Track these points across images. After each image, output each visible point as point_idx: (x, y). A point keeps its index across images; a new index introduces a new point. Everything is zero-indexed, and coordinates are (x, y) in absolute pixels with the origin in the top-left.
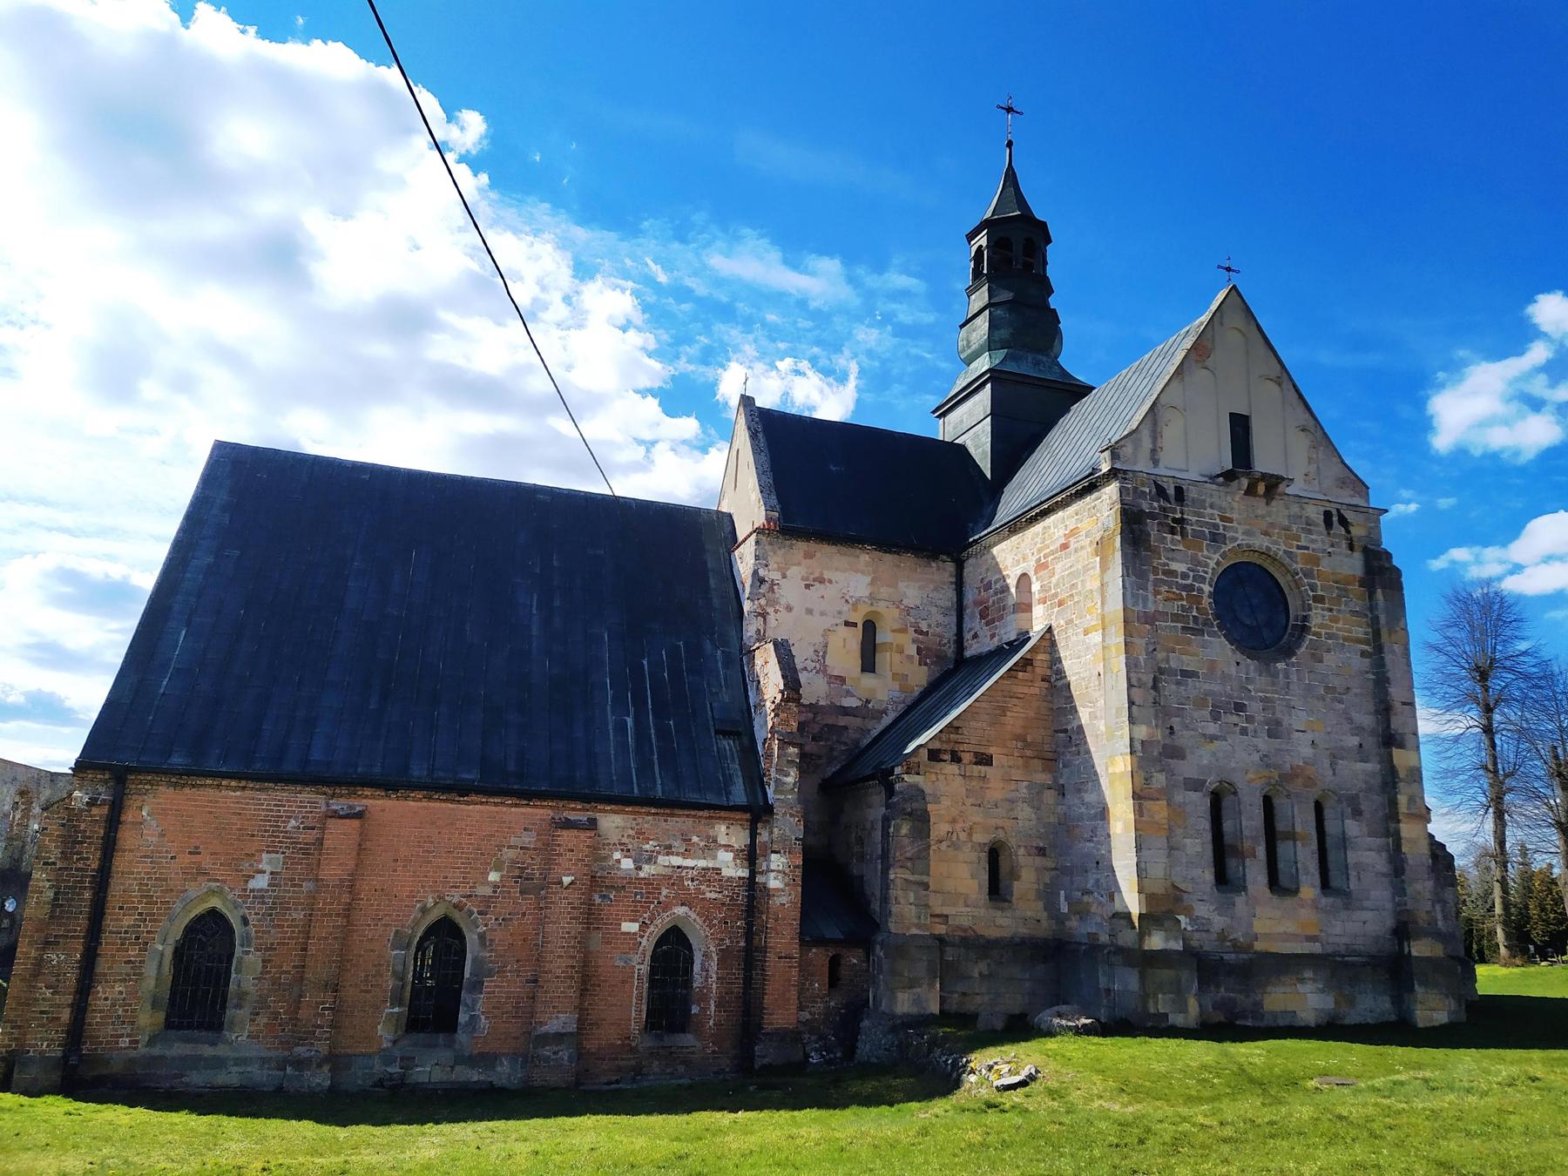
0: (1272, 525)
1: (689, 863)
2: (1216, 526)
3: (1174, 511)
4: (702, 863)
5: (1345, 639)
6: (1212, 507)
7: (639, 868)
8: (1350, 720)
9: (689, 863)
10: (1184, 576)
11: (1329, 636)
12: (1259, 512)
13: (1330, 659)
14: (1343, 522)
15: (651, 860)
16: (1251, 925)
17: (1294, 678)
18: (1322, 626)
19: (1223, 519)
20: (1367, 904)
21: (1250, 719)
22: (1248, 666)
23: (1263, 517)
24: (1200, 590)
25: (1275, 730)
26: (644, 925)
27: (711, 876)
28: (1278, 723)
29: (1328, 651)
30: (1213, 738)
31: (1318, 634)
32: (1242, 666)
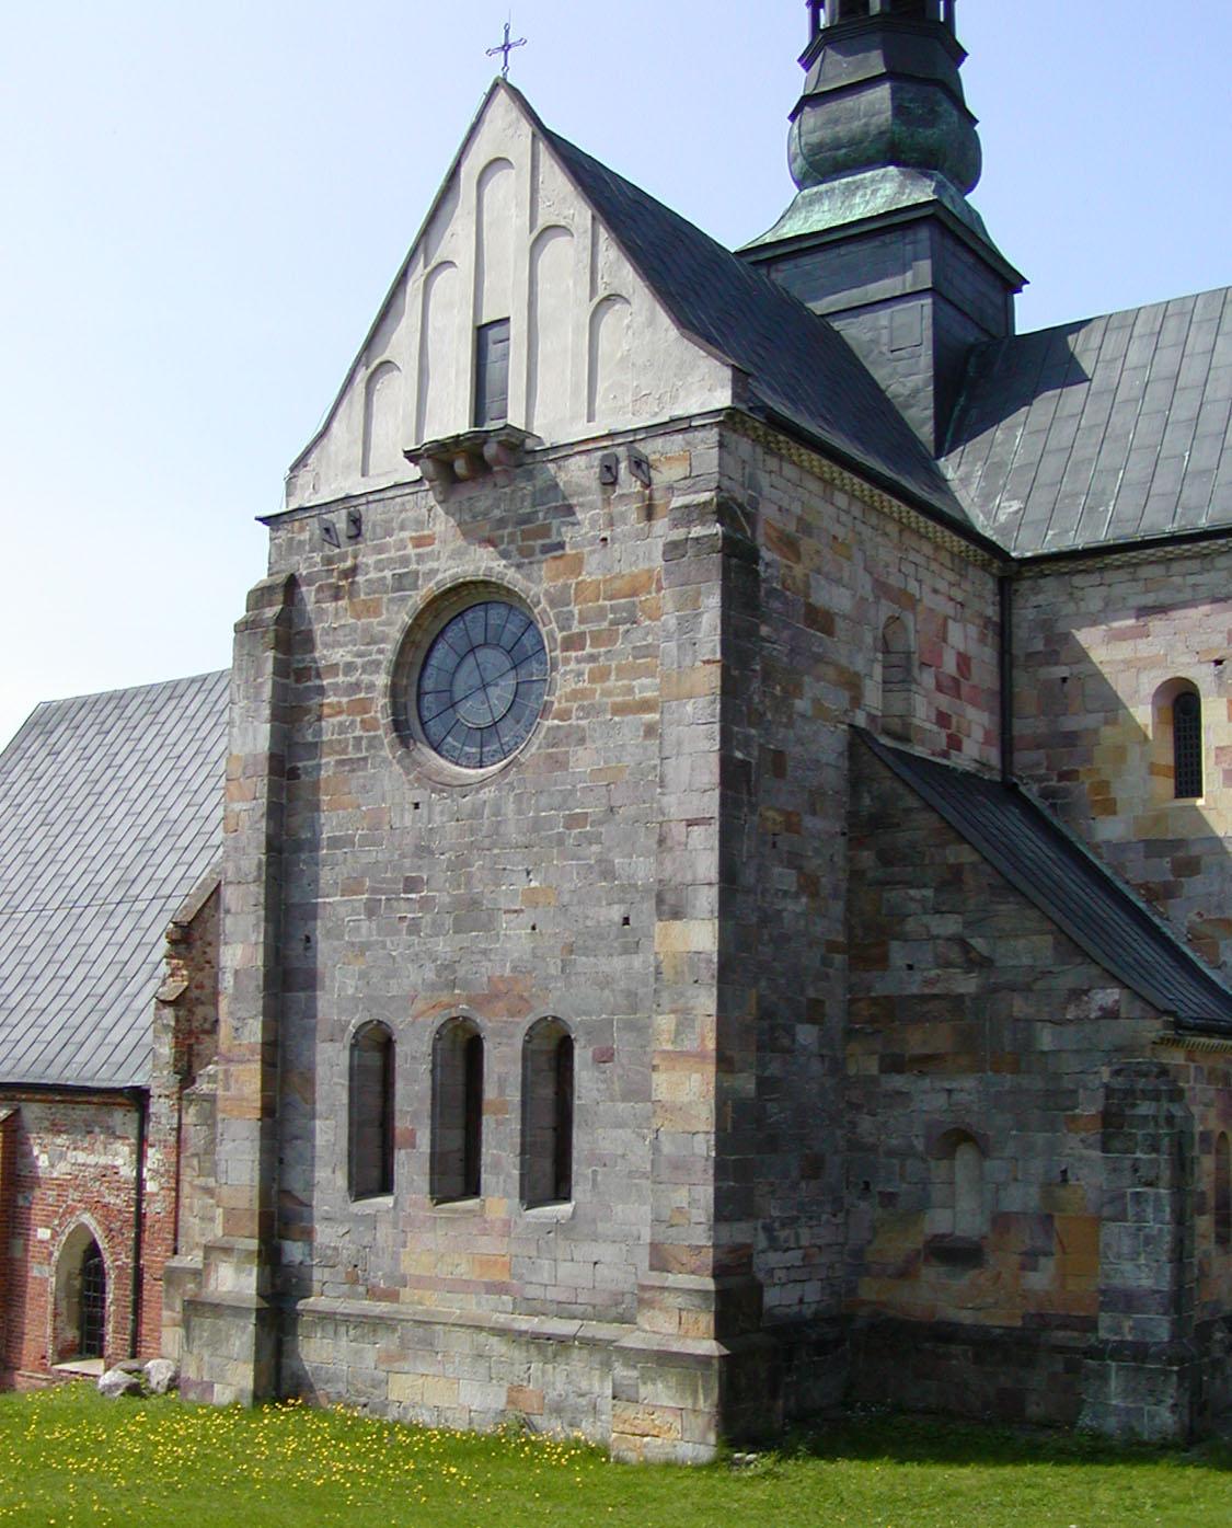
0: (502, 523)
1: (92, 1160)
2: (405, 561)
3: (343, 558)
4: (103, 1160)
5: (619, 710)
6: (402, 528)
7: (52, 1166)
8: (608, 873)
9: (92, 1160)
10: (349, 668)
11: (588, 712)
12: (482, 505)
13: (583, 760)
14: (640, 464)
15: (62, 1157)
16: (395, 1257)
17: (510, 808)
18: (575, 695)
19: (419, 542)
20: (601, 1227)
21: (425, 904)
22: (430, 805)
23: (485, 514)
24: (371, 687)
25: (472, 915)
26: (55, 1234)
27: (107, 1174)
28: (474, 903)
29: (582, 741)
30: (364, 948)
31: (564, 715)
32: (423, 809)
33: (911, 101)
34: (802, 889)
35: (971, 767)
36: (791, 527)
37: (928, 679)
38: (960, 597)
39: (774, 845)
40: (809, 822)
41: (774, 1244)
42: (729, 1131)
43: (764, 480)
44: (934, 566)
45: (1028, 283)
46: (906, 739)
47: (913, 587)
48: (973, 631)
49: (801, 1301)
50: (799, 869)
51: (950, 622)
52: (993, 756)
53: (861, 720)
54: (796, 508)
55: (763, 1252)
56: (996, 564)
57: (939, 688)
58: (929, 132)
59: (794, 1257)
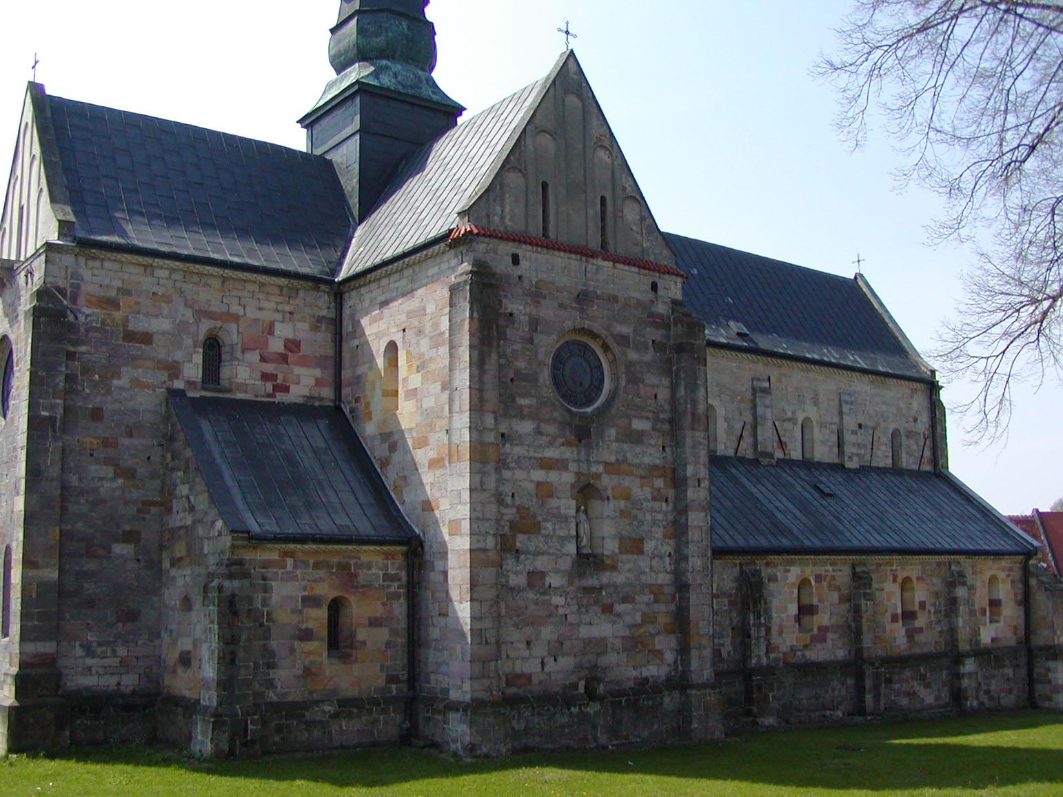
33: (369, 24)
34: (116, 476)
35: (300, 400)
36: (113, 294)
37: (254, 357)
38: (288, 308)
39: (91, 455)
40: (125, 441)
41: (90, 653)
42: (34, 596)
43: (87, 274)
44: (262, 296)
45: (465, 109)
46: (229, 391)
47: (235, 309)
48: (304, 326)
49: (119, 684)
50: (117, 466)
51: (277, 324)
52: (327, 393)
53: (179, 384)
54: (118, 283)
55: (81, 657)
56: (323, 287)
57: (263, 359)
58: (379, 40)
59: (114, 662)
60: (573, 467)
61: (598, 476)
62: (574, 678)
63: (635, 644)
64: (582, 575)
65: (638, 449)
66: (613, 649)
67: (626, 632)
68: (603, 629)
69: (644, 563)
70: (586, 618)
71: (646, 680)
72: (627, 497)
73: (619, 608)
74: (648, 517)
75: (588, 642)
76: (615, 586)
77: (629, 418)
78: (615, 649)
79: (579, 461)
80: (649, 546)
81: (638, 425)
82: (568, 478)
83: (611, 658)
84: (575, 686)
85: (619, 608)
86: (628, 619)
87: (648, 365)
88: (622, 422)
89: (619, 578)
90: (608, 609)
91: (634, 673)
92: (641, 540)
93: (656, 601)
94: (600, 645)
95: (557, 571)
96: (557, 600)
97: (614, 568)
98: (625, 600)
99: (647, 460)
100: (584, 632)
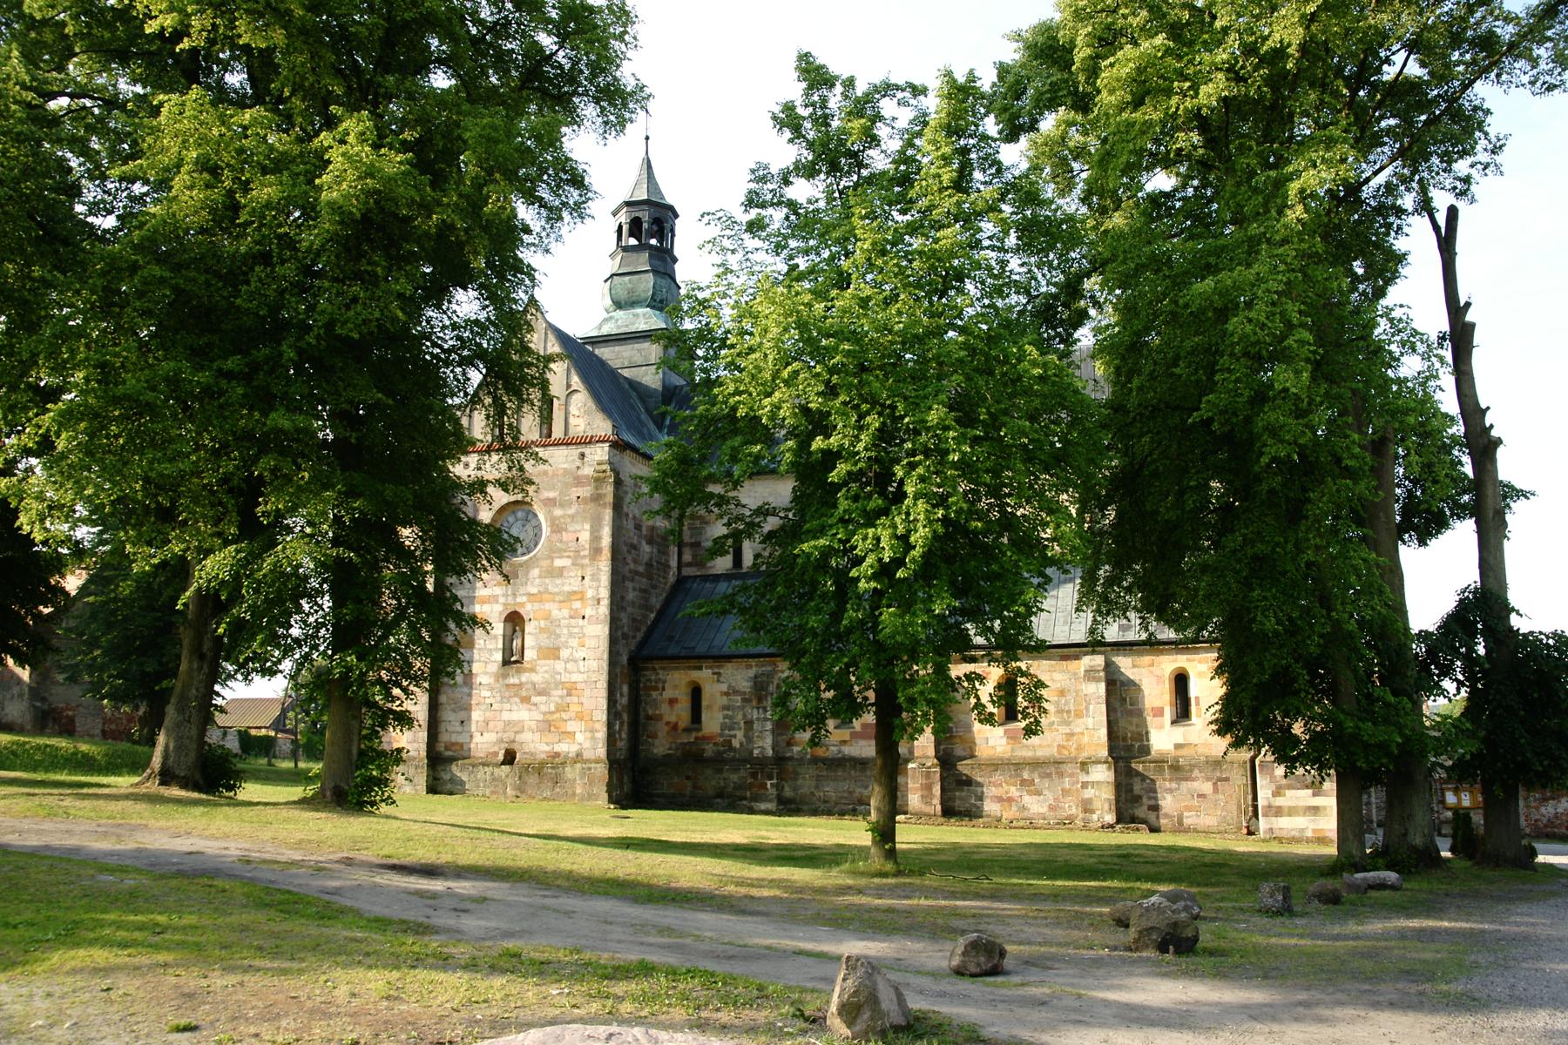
60: (502, 600)
61: (522, 605)
62: (496, 749)
63: (547, 726)
64: (505, 676)
65: (558, 581)
66: (530, 729)
67: (541, 717)
68: (522, 714)
69: (559, 666)
70: (507, 706)
71: (557, 755)
72: (548, 617)
73: (535, 699)
74: (565, 631)
75: (508, 723)
76: (534, 684)
77: (552, 559)
78: (530, 729)
79: (506, 595)
80: (564, 653)
81: (558, 563)
82: (498, 608)
83: (526, 737)
84: (496, 754)
85: (535, 699)
86: (543, 708)
87: (573, 517)
88: (545, 563)
89: (536, 678)
90: (526, 700)
91: (547, 748)
92: (558, 649)
93: (569, 694)
94: (519, 727)
95: (486, 673)
96: (488, 694)
97: (533, 670)
98: (540, 694)
99: (566, 588)
100: (506, 716)
